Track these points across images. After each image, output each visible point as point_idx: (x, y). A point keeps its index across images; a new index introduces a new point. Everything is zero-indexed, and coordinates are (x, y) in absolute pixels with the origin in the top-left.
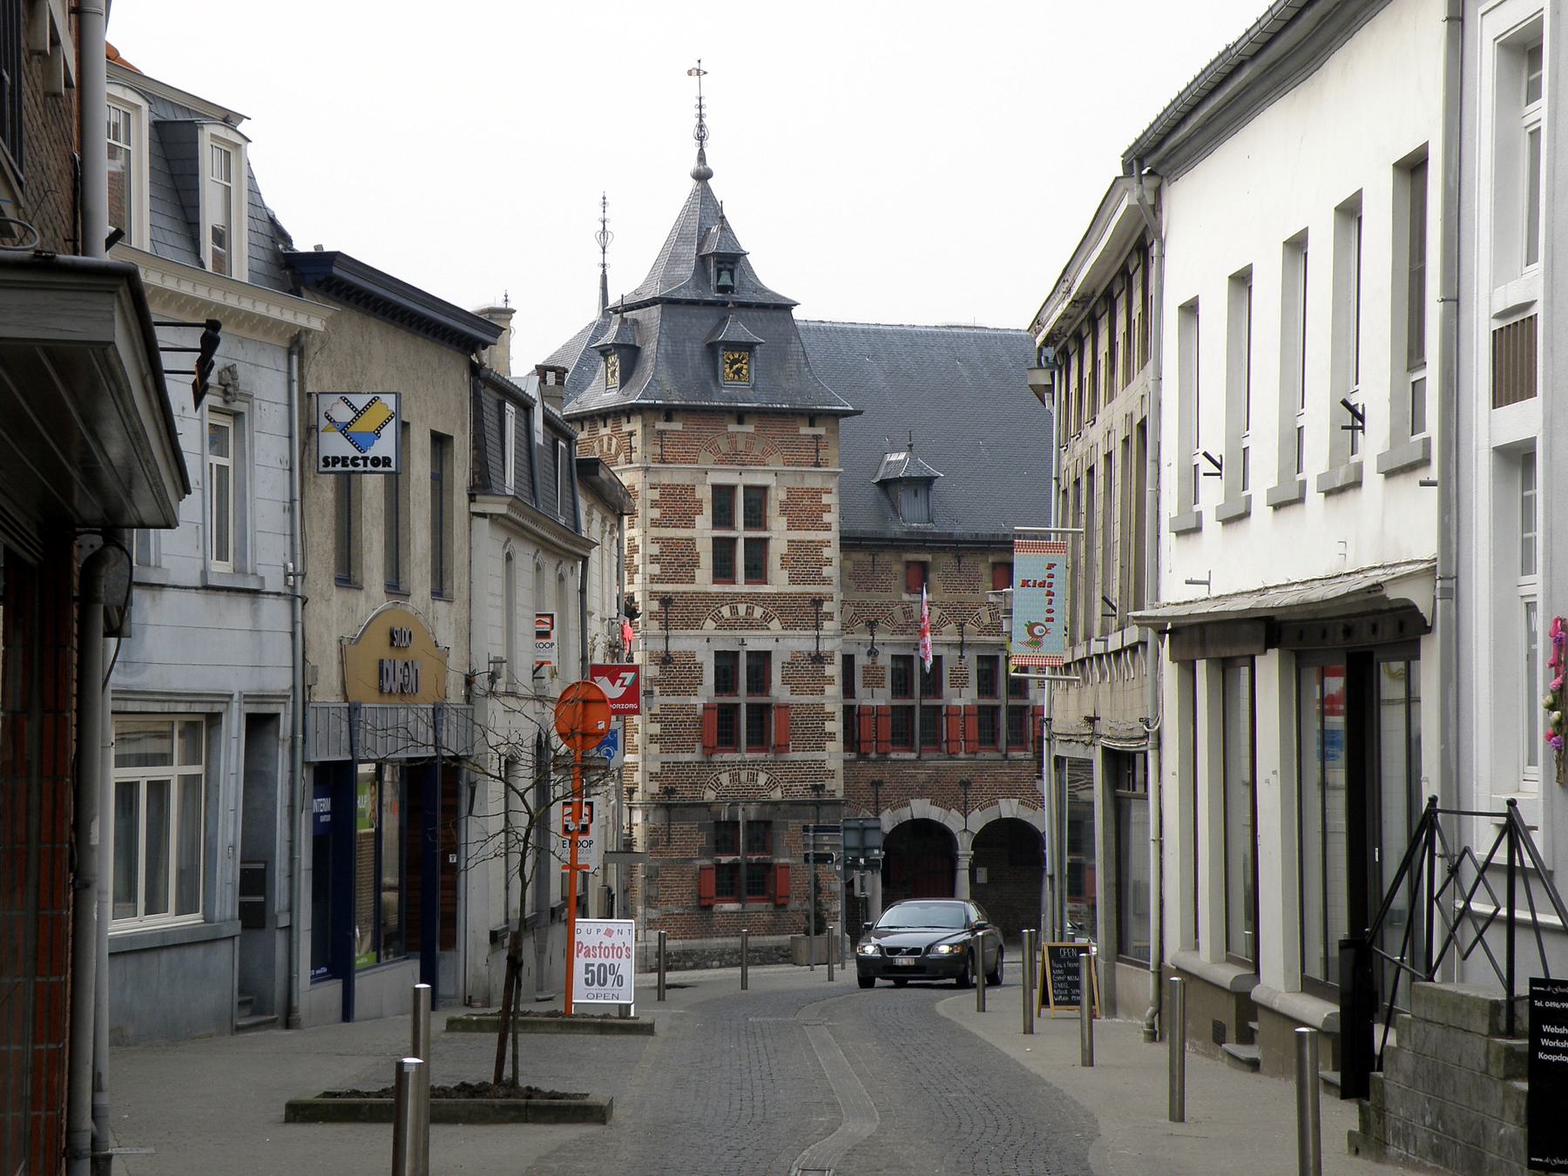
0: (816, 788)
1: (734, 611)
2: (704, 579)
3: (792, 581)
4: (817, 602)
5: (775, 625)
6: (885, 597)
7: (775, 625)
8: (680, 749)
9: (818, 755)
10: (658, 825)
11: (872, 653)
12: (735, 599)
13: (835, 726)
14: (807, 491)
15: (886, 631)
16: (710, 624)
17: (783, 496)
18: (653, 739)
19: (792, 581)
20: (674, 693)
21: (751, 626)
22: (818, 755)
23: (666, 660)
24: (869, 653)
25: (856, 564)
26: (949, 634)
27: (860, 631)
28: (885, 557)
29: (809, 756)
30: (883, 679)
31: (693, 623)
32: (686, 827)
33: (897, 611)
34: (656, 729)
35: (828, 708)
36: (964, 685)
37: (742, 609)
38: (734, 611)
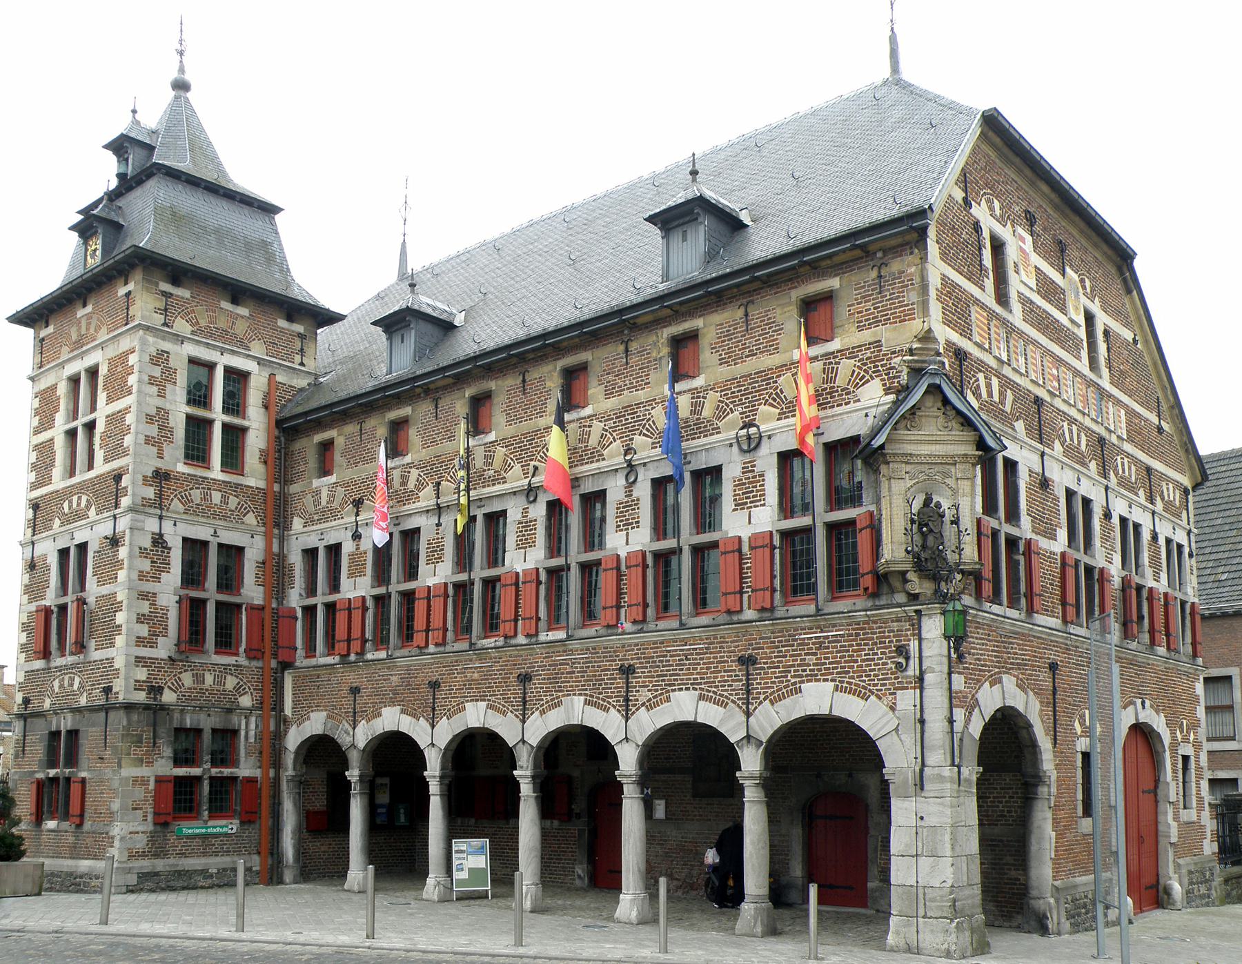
36: (440, 559)
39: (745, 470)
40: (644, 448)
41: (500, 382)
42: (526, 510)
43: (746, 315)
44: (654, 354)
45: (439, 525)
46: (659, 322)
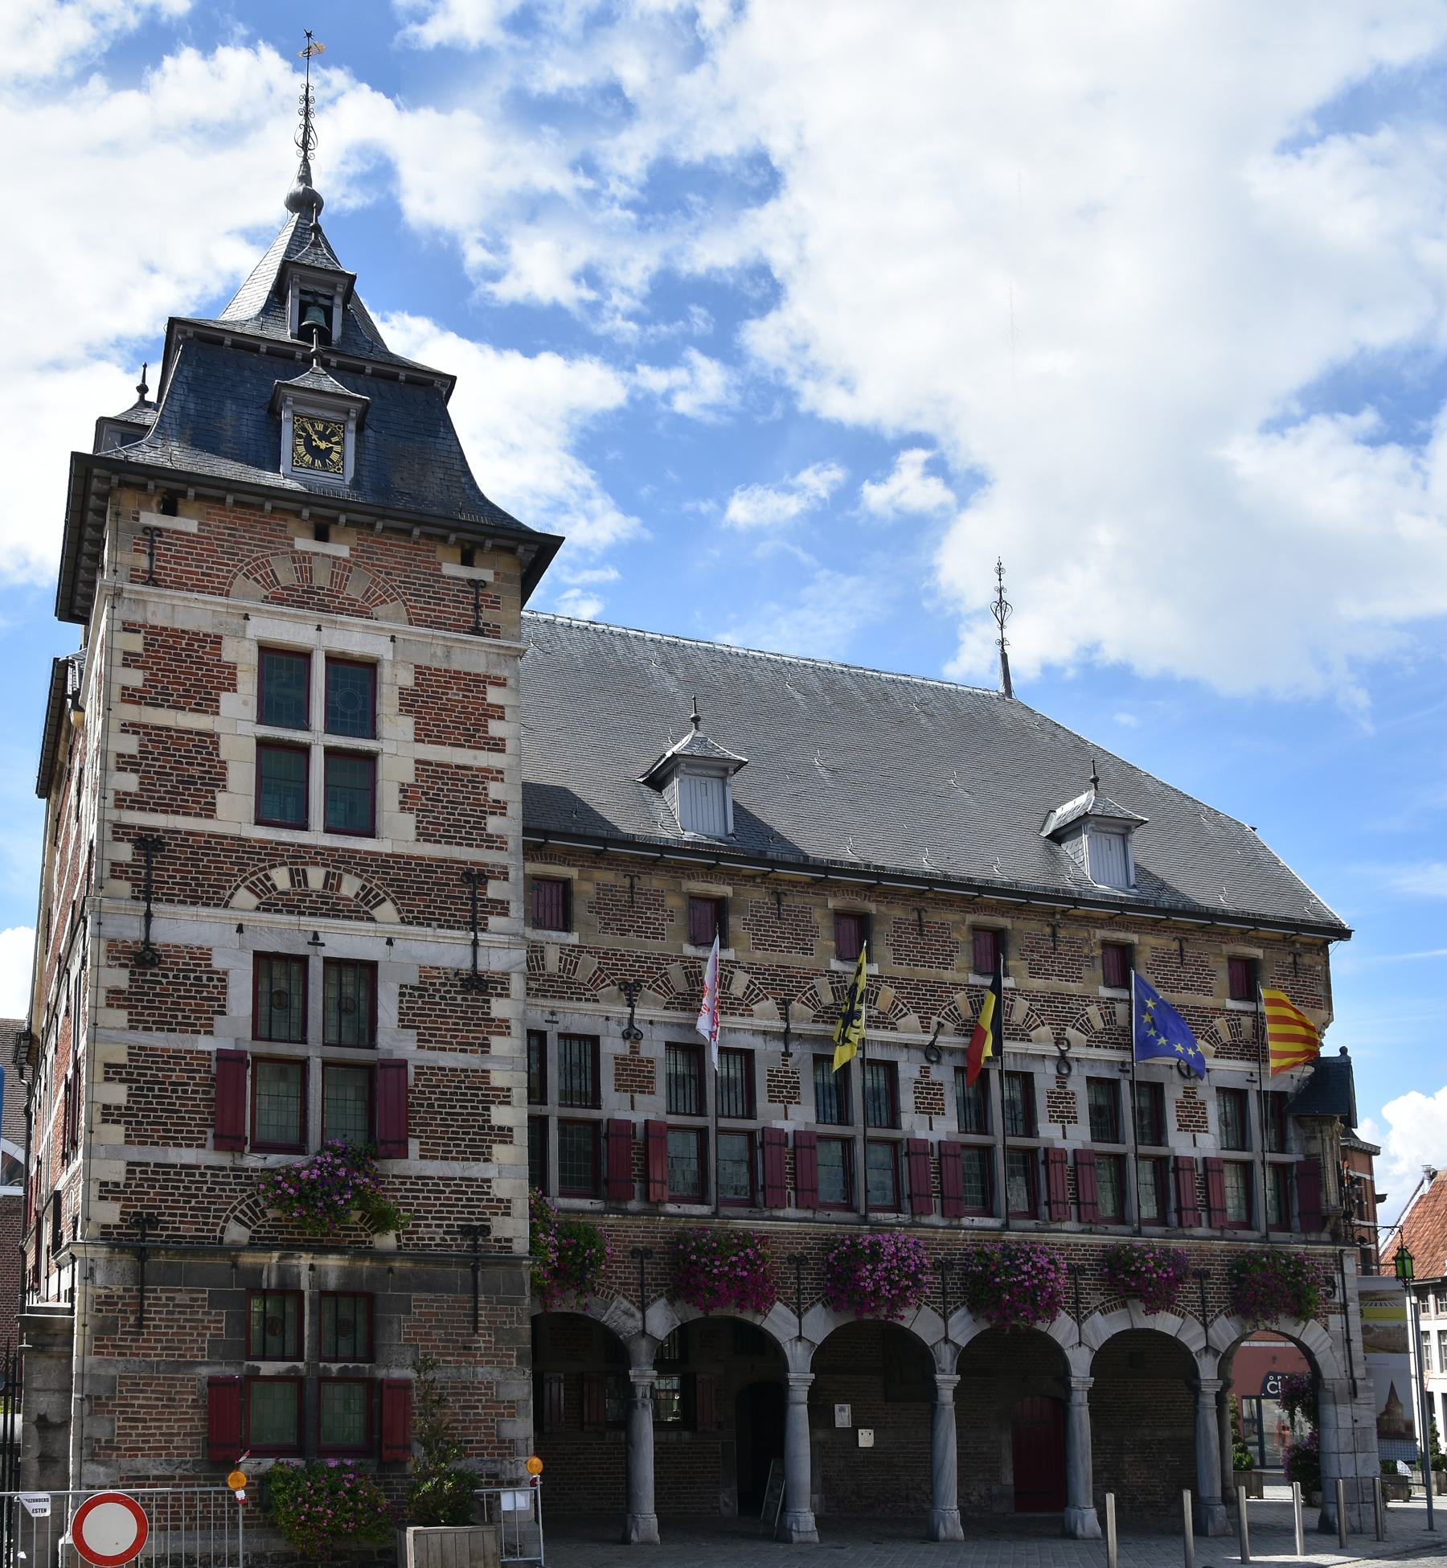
0: (467, 1231)
1: (299, 878)
2: (234, 812)
3: (423, 835)
4: (476, 877)
5: (387, 911)
6: (654, 947)
7: (387, 911)
8: (167, 1140)
9: (476, 1170)
10: (117, 1289)
11: (631, 1034)
12: (298, 858)
13: (511, 1116)
14: (457, 676)
15: (655, 1002)
16: (244, 898)
17: (407, 679)
18: (109, 1114)
19: (423, 835)
20: (162, 1025)
21: (334, 912)
22: (476, 1170)
23: (143, 957)
24: (626, 1036)
25: (602, 888)
26: (763, 1016)
27: (611, 1000)
28: (654, 882)
29: (455, 1169)
30: (650, 1079)
31: (207, 893)
32: (182, 1298)
33: (675, 971)
34: (118, 1094)
35: (498, 1079)
37: (316, 877)
38: (299, 878)
39: (1187, 1095)
40: (1079, 1044)
41: (883, 909)
42: (925, 1071)
43: (1181, 949)
44: (1086, 951)
45: (787, 1054)
46: (1109, 922)
